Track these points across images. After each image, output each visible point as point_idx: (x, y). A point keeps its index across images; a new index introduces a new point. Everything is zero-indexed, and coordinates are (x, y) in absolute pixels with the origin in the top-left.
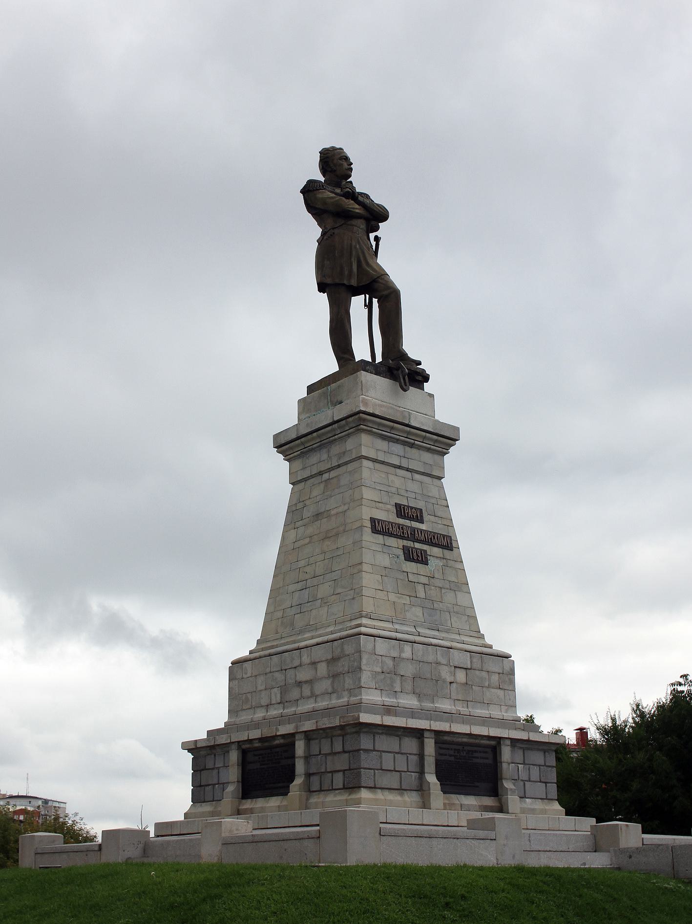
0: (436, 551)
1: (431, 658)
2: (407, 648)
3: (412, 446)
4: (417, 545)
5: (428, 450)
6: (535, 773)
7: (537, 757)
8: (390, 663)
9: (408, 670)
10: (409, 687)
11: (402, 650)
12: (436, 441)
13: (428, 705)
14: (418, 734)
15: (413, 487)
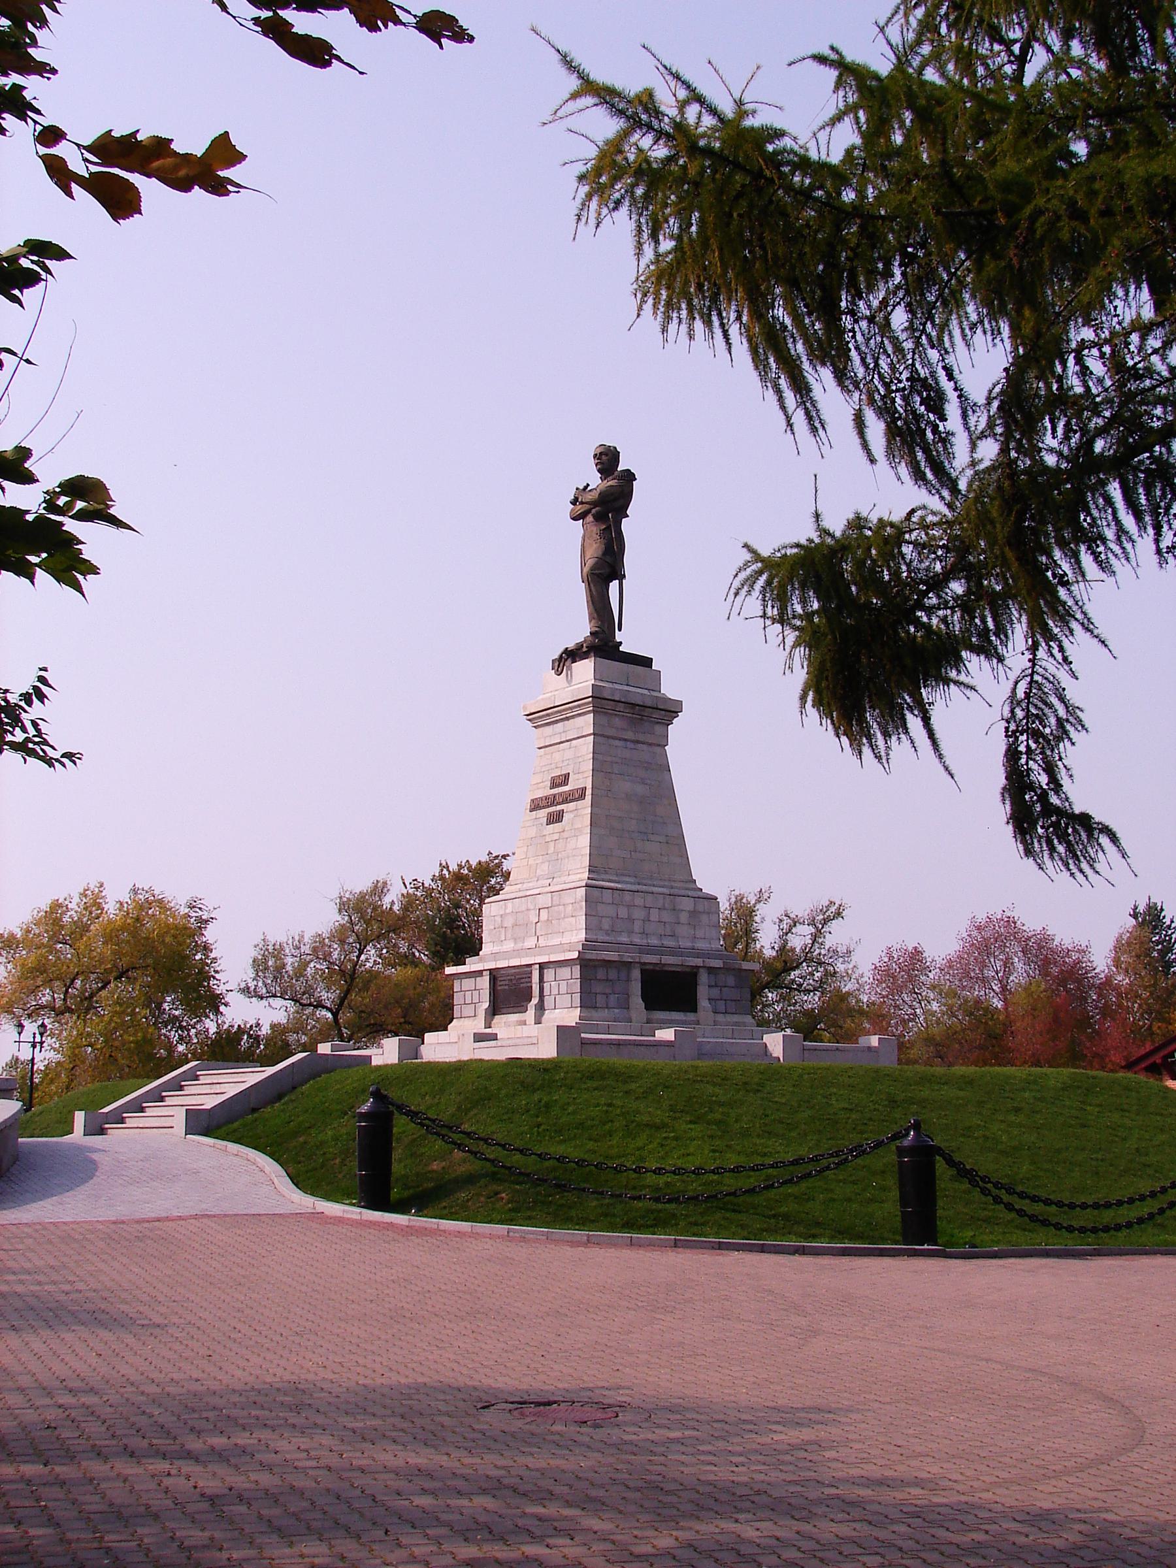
0: (572, 805)
1: (523, 908)
2: (509, 903)
3: (567, 719)
4: (559, 808)
5: (580, 715)
6: (563, 989)
7: (565, 972)
8: (498, 919)
9: (509, 922)
10: (509, 936)
11: (506, 907)
12: (579, 706)
13: (519, 945)
14: (480, 973)
15: (569, 754)
